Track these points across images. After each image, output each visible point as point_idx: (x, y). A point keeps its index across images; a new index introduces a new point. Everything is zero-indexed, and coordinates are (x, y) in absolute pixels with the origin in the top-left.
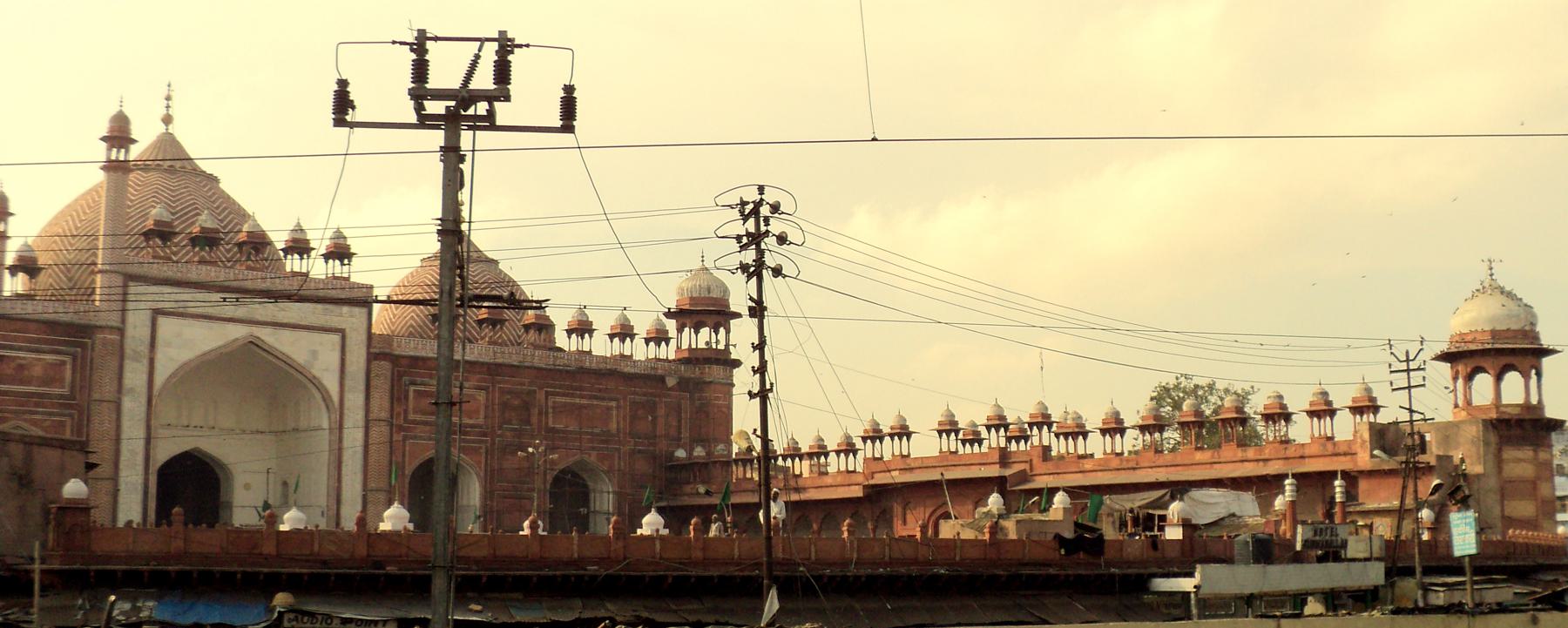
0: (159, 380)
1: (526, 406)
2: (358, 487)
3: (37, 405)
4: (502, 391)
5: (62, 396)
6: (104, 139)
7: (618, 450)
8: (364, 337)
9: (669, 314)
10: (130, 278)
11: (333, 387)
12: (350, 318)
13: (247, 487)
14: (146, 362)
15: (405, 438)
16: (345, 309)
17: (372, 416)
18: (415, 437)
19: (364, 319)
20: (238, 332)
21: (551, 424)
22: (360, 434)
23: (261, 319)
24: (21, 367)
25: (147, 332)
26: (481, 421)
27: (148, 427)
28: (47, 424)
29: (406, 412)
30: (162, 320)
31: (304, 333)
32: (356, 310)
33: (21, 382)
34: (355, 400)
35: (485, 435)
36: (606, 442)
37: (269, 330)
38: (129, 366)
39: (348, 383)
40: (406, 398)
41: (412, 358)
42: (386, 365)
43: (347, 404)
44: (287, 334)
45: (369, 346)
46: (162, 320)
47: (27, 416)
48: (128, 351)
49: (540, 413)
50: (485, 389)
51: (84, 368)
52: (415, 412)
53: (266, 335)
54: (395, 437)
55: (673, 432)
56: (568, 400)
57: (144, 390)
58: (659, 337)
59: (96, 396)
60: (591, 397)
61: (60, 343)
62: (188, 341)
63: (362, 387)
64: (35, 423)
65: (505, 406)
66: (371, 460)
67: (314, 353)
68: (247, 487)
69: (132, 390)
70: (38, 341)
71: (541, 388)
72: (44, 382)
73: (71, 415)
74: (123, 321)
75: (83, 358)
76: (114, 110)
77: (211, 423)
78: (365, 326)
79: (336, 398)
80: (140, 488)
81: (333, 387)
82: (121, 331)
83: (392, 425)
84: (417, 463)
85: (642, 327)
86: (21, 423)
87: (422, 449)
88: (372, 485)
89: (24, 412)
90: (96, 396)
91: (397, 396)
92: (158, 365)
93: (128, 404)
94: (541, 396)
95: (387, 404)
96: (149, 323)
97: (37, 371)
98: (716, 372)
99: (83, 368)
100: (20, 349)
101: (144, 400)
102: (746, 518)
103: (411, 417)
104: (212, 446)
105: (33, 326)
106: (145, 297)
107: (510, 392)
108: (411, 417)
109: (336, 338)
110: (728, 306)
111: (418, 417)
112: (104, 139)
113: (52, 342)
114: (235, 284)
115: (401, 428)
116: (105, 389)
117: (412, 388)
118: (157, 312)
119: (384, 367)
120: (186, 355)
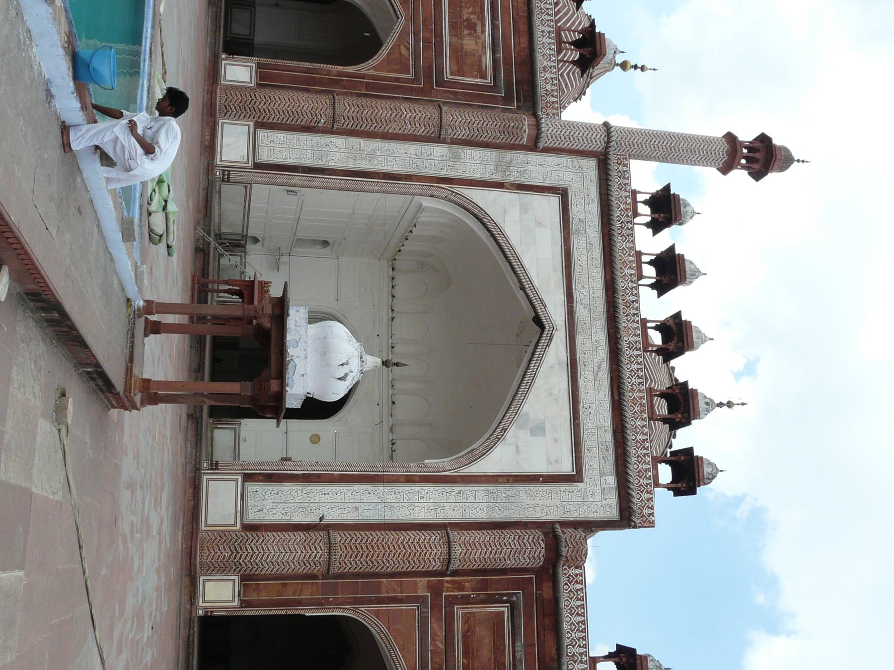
0: (477, 196)
2: (332, 516)
5: (440, 71)
11: (489, 465)
12: (597, 496)
13: (315, 439)
14: (497, 178)
15: (421, 600)
17: (454, 535)
18: (423, 621)
22: (421, 515)
23: (579, 340)
24: (472, 27)
27: (408, 177)
28: (404, 51)
30: (554, 201)
32: (613, 500)
33: (453, 26)
34: (475, 504)
38: (491, 155)
39: (503, 490)
40: (491, 600)
41: (556, 600)
42: (540, 550)
45: (565, 524)
47: (411, 28)
48: (509, 155)
51: (477, 98)
52: (467, 618)
53: (556, 352)
54: (422, 581)
59: (444, 108)
61: (508, 74)
62: (531, 233)
63: (499, 516)
64: (403, 35)
66: (377, 535)
67: (538, 430)
68: (315, 439)
69: (457, 158)
70: (507, 48)
72: (458, 54)
73: (416, 79)
74: (547, 150)
75: (493, 99)
77: (398, 385)
79: (476, 469)
80: (321, 164)
82: (534, 146)
83: (442, 574)
88: (337, 537)
89: (416, 26)
91: (489, 580)
93: (439, 151)
96: (548, 183)
97: (469, 44)
99: (479, 97)
100: (494, 27)
101: (444, 173)
103: (459, 611)
105: (524, 41)
106: (580, 177)
108: (459, 611)
109: (566, 467)
111: (458, 625)
113: (508, 62)
115: (436, 590)
116: (459, 120)
117: (505, 609)
118: (563, 193)
119: (529, 552)
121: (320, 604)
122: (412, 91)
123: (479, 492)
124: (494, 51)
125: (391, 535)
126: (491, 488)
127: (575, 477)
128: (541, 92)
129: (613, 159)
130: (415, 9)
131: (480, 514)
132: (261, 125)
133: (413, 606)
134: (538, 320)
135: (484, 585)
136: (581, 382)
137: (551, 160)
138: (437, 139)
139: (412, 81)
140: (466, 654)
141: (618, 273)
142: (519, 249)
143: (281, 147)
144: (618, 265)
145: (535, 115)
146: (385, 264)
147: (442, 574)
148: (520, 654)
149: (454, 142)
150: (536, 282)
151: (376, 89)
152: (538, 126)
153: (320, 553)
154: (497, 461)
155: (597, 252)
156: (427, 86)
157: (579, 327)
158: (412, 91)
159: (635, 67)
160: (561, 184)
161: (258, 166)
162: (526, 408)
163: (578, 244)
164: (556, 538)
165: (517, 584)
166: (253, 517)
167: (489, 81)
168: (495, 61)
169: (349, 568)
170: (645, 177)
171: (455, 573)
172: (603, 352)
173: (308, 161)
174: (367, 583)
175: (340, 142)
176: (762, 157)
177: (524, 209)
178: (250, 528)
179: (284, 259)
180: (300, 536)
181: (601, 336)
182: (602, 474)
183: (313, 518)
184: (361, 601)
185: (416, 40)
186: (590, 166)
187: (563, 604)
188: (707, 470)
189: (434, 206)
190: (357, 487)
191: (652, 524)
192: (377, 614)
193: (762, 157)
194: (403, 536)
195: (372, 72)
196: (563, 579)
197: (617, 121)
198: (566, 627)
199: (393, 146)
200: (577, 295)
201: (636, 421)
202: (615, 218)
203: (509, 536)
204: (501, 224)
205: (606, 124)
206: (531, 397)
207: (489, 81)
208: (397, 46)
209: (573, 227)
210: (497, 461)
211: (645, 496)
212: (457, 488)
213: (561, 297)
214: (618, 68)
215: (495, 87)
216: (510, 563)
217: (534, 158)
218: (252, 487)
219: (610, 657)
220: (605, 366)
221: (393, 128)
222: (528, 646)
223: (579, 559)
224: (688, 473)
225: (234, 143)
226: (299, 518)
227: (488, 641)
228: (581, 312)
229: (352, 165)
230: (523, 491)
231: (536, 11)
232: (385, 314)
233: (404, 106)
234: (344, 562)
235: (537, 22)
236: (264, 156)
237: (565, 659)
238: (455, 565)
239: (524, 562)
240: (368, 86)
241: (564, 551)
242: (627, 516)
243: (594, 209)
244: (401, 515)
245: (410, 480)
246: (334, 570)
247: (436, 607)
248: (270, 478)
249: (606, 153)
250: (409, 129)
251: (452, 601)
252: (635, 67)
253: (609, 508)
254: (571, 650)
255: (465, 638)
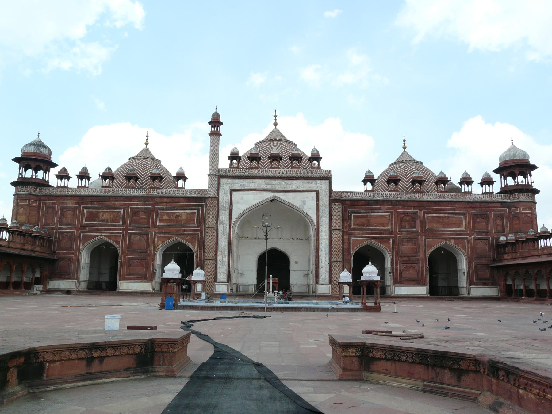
0: (234, 217)
1: (414, 220)
2: (327, 261)
3: (184, 231)
4: (399, 213)
5: (194, 227)
6: (210, 123)
7: (467, 238)
8: (328, 193)
9: (496, 171)
10: (221, 177)
11: (313, 216)
12: (322, 186)
13: (296, 262)
14: (228, 211)
16: (318, 182)
17: (333, 228)
19: (328, 185)
20: (269, 195)
21: (428, 228)
22: (327, 236)
23: (277, 188)
24: (178, 216)
25: (228, 198)
26: (389, 227)
27: (230, 238)
28: (188, 238)
29: (350, 225)
30: (235, 193)
31: (299, 194)
32: (323, 182)
33: (178, 222)
35: (391, 234)
36: (460, 235)
37: (282, 193)
39: (321, 214)
40: (350, 218)
41: (350, 200)
43: (320, 223)
44: (290, 195)
45: (330, 196)
46: (235, 193)
47: (180, 235)
48: (220, 206)
49: (421, 222)
50: (391, 212)
51: (202, 215)
55: (500, 228)
56: (435, 215)
57: (228, 222)
58: (487, 181)
59: (207, 226)
60: (449, 213)
61: (193, 205)
62: (245, 202)
63: (328, 215)
65: (401, 220)
67: (304, 202)
68: (296, 262)
69: (222, 223)
71: (421, 210)
72: (188, 221)
73: (198, 234)
74: (218, 194)
75: (202, 210)
76: (214, 112)
77: (280, 237)
78: (328, 188)
81: (313, 216)
82: (217, 199)
83: (343, 231)
84: (356, 250)
85: (477, 178)
86: (177, 238)
87: (359, 242)
88: (333, 259)
90: (207, 226)
91: (345, 219)
92: (233, 212)
93: (220, 228)
94: (420, 214)
95: (339, 222)
97: (184, 217)
98: (523, 197)
99: (202, 215)
100: (177, 209)
101: (228, 227)
102: (536, 271)
103: (353, 227)
104: (280, 246)
105: (181, 199)
106: (226, 185)
107: (404, 213)
108: (353, 227)
109: (314, 195)
110: (529, 162)
111: (356, 227)
112: (210, 123)
114: (266, 175)
115: (347, 233)
116: (210, 222)
118: (232, 190)
119: (338, 207)
120: (245, 207)
121: (350, 264)
122: (201, 236)
123: (321, 220)
124: (186, 209)
125: (333, 245)
126: (320, 217)
127: (317, 192)
128: (199, 195)
129: (220, 174)
130: (173, 234)
131: (327, 220)
132: (215, 281)
133: (351, 239)
134: (272, 201)
135: (346, 220)
136: (290, 189)
137: (221, 193)
138: (217, 229)
139: (198, 236)
140: (363, 226)
141: (257, 175)
142: (251, 205)
143: (222, 274)
144: (254, 175)
145: (207, 198)
146: (240, 241)
147: (343, 231)
148: (364, 211)
149: (217, 224)
150: (260, 201)
151: (201, 246)
152: (212, 198)
153: (337, 264)
154: (313, 215)
155: (251, 181)
156: (199, 231)
157: (274, 188)
158: (201, 236)
159: (147, 139)
160: (229, 191)
161: (228, 281)
162: (298, 206)
163: (248, 187)
164: (334, 200)
165: (346, 211)
166: (328, 282)
167: (196, 212)
168: (189, 209)
169: (341, 256)
170: (224, 163)
171: (343, 228)
172: (281, 181)
173: (226, 267)
174: (345, 251)
175: (219, 258)
176: (216, 122)
177: (238, 203)
178: (330, 283)
179: (240, 272)
180: (333, 269)
181: (276, 182)
182: (316, 184)
183: (328, 266)
184: (350, 253)
185: (184, 234)
186: (223, 181)
187: (351, 198)
188: (315, 152)
189: (236, 230)
190: (320, 254)
191: (330, 171)
192: (353, 249)
193: (216, 122)
194: (333, 242)
195: (196, 248)
196: (345, 198)
197: (207, 172)
198: (357, 198)
199: (219, 242)
200: (264, 188)
201: (301, 173)
202: (240, 175)
203: (333, 213)
204: (243, 210)
205: (209, 175)
206: (295, 204)
207: (196, 212)
208: (187, 240)
209: (243, 188)
210: (313, 215)
211: (323, 172)
212: (320, 226)
213: (265, 193)
214: (148, 146)
215: (199, 210)
216: (341, 213)
217: (221, 199)
218: (320, 282)
219: (365, 184)
220: (285, 181)
221: (214, 242)
222: (362, 209)
223: (339, 193)
224: (316, 157)
225: (222, 288)
226: (328, 270)
227: (360, 219)
228: (269, 187)
229: (227, 254)
230: (321, 208)
231: (170, 195)
232: (257, 240)
233: (207, 238)
234: (340, 258)
235: (174, 195)
236: (225, 280)
237: (366, 199)
238: (341, 228)
239: (340, 209)
240: (201, 249)
241: (338, 198)
242: (327, 178)
243: (236, 181)
244: (327, 242)
245: (318, 240)
246: (341, 260)
247: (351, 233)
248: (317, 277)
249: (218, 176)
250: (214, 237)
251: (350, 229)
252: (147, 139)
253: (325, 183)
254: (363, 197)
255: (360, 225)
